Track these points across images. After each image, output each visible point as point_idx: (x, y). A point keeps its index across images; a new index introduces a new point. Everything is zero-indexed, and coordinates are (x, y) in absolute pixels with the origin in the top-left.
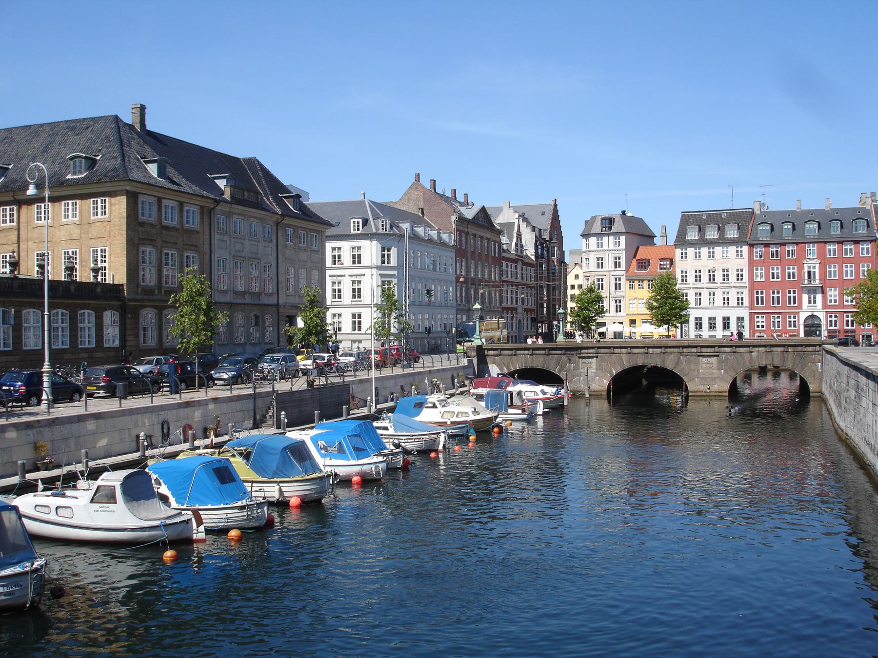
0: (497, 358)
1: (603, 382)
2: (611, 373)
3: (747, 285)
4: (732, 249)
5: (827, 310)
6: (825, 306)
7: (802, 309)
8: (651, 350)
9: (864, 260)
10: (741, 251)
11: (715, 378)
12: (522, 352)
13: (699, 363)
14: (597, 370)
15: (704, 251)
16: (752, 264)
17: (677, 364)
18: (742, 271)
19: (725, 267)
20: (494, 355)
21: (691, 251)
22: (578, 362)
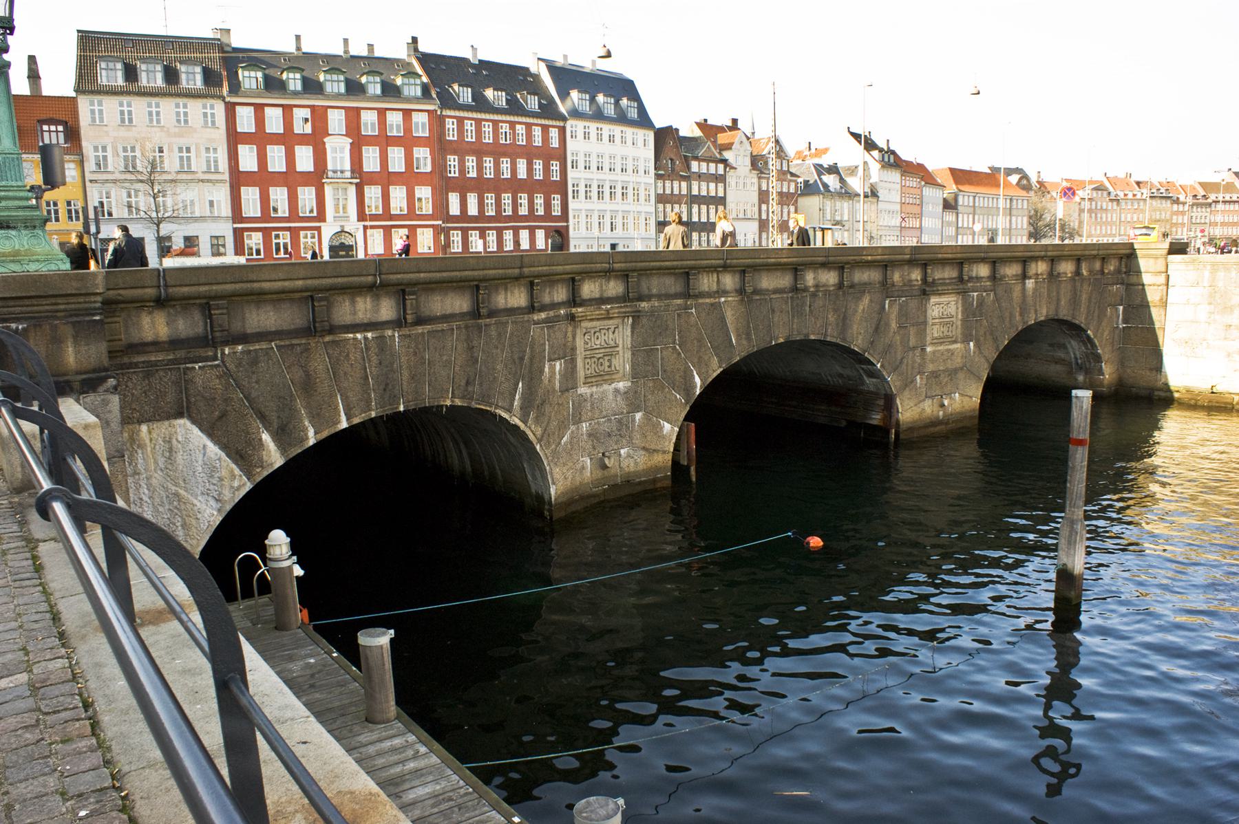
0: (202, 374)
1: (657, 429)
2: (688, 387)
3: (227, 177)
4: (195, 108)
5: (368, 223)
6: (362, 216)
7: (324, 220)
8: (810, 278)
9: (420, 142)
10: (213, 115)
11: (956, 371)
12: (363, 308)
13: (925, 323)
14: (635, 375)
15: (139, 106)
16: (235, 138)
17: (877, 329)
18: (215, 150)
19: (184, 142)
20: (175, 343)
21: (111, 105)
22: (574, 349)
